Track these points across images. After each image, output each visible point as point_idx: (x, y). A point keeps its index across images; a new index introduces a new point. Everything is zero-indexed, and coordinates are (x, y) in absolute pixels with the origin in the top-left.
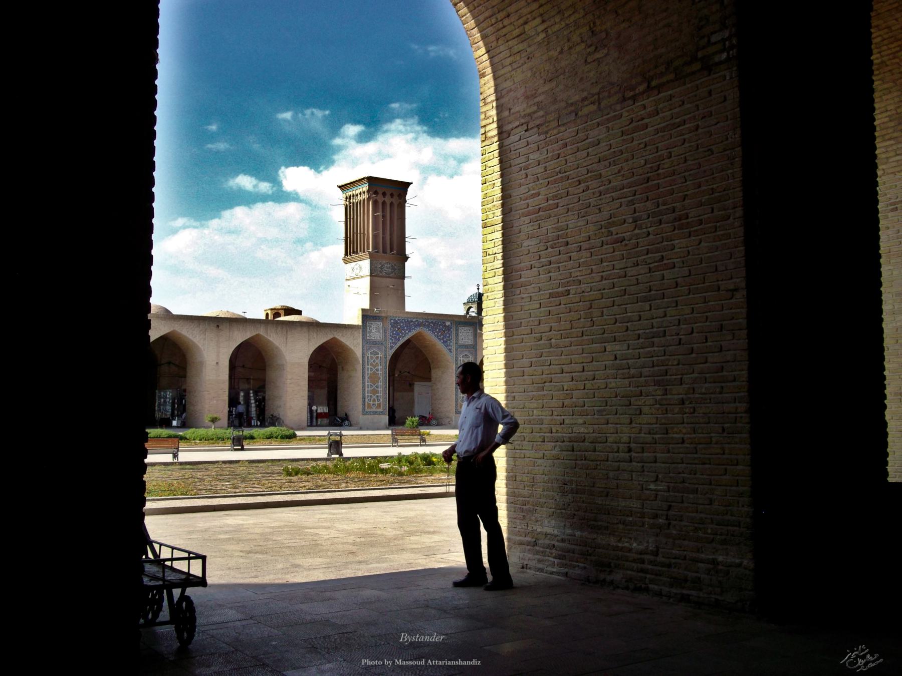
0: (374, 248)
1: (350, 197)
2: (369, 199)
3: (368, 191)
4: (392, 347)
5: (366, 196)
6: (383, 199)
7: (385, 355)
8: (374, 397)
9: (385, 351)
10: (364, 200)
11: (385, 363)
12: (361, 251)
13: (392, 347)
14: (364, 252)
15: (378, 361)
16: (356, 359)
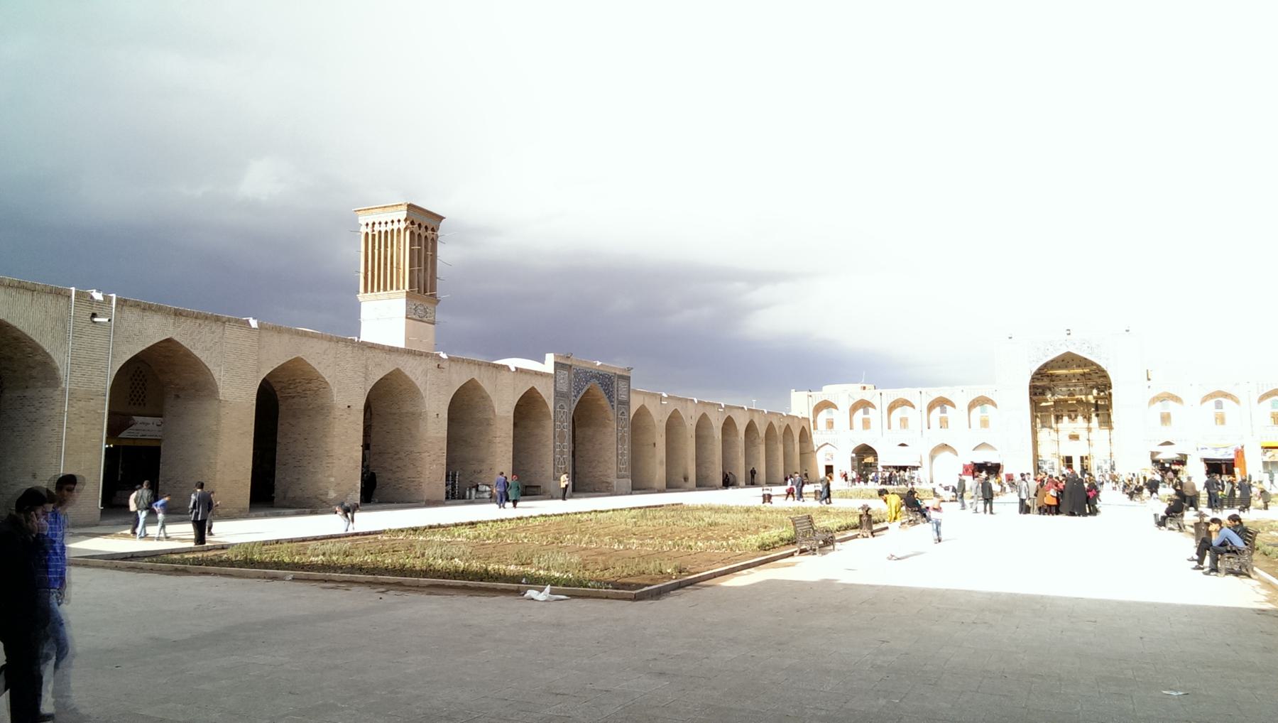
0: (411, 287)
1: (374, 224)
2: (406, 229)
3: (406, 220)
4: (574, 400)
5: (403, 225)
6: (421, 232)
7: (570, 409)
8: (562, 459)
9: (570, 405)
10: (393, 230)
11: (569, 418)
12: (392, 288)
13: (574, 400)
14: (398, 288)
15: (564, 417)
16: (548, 414)
